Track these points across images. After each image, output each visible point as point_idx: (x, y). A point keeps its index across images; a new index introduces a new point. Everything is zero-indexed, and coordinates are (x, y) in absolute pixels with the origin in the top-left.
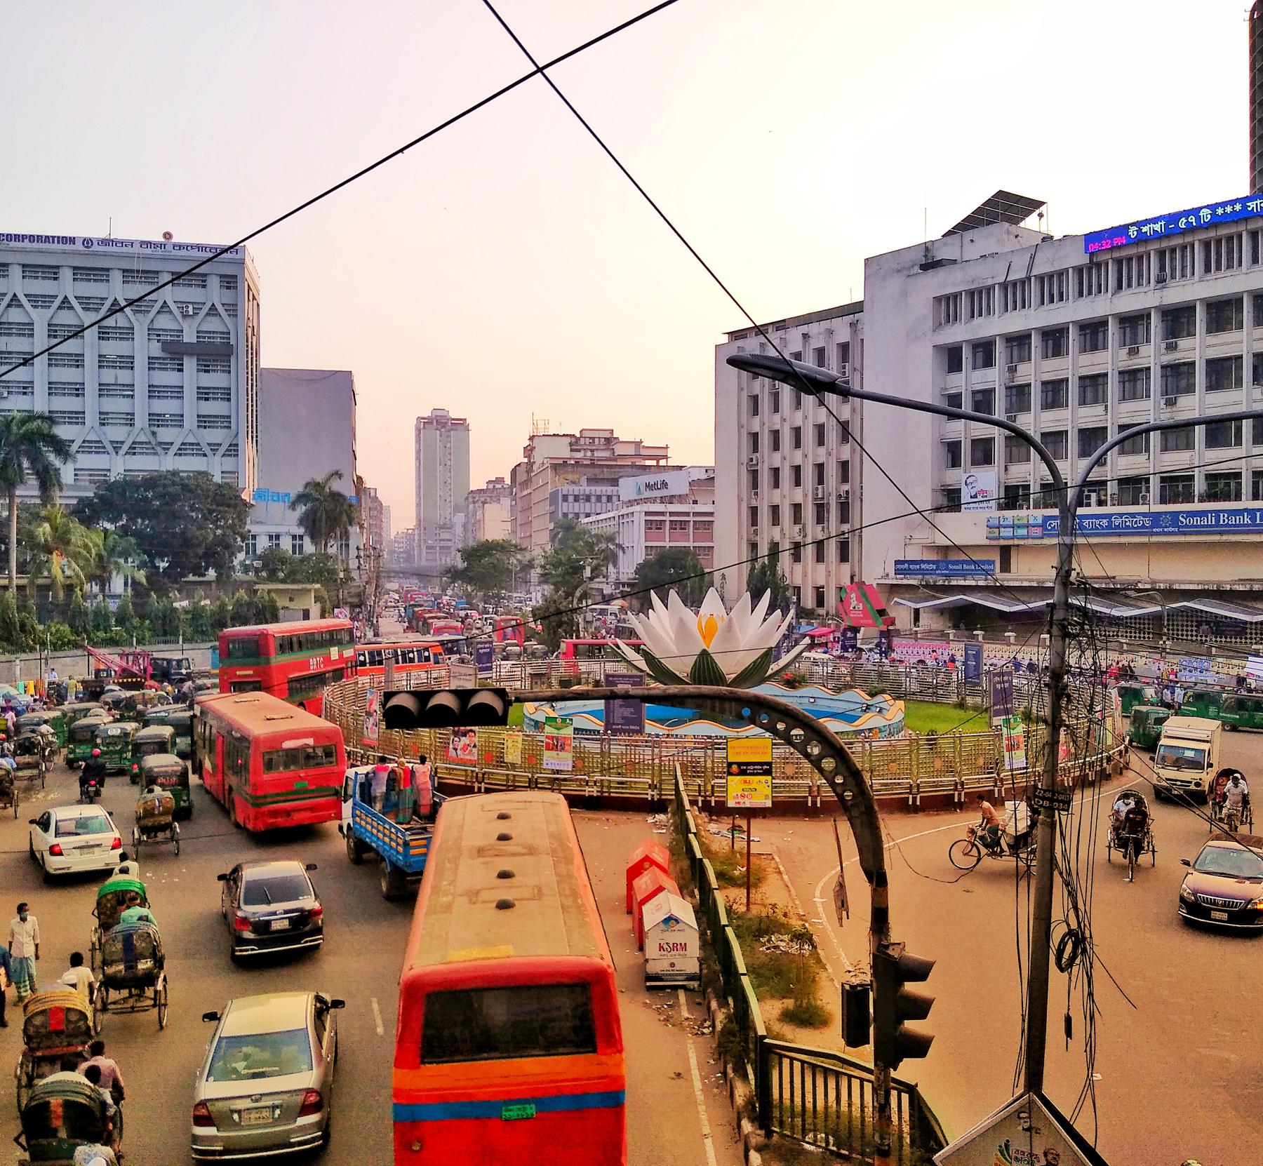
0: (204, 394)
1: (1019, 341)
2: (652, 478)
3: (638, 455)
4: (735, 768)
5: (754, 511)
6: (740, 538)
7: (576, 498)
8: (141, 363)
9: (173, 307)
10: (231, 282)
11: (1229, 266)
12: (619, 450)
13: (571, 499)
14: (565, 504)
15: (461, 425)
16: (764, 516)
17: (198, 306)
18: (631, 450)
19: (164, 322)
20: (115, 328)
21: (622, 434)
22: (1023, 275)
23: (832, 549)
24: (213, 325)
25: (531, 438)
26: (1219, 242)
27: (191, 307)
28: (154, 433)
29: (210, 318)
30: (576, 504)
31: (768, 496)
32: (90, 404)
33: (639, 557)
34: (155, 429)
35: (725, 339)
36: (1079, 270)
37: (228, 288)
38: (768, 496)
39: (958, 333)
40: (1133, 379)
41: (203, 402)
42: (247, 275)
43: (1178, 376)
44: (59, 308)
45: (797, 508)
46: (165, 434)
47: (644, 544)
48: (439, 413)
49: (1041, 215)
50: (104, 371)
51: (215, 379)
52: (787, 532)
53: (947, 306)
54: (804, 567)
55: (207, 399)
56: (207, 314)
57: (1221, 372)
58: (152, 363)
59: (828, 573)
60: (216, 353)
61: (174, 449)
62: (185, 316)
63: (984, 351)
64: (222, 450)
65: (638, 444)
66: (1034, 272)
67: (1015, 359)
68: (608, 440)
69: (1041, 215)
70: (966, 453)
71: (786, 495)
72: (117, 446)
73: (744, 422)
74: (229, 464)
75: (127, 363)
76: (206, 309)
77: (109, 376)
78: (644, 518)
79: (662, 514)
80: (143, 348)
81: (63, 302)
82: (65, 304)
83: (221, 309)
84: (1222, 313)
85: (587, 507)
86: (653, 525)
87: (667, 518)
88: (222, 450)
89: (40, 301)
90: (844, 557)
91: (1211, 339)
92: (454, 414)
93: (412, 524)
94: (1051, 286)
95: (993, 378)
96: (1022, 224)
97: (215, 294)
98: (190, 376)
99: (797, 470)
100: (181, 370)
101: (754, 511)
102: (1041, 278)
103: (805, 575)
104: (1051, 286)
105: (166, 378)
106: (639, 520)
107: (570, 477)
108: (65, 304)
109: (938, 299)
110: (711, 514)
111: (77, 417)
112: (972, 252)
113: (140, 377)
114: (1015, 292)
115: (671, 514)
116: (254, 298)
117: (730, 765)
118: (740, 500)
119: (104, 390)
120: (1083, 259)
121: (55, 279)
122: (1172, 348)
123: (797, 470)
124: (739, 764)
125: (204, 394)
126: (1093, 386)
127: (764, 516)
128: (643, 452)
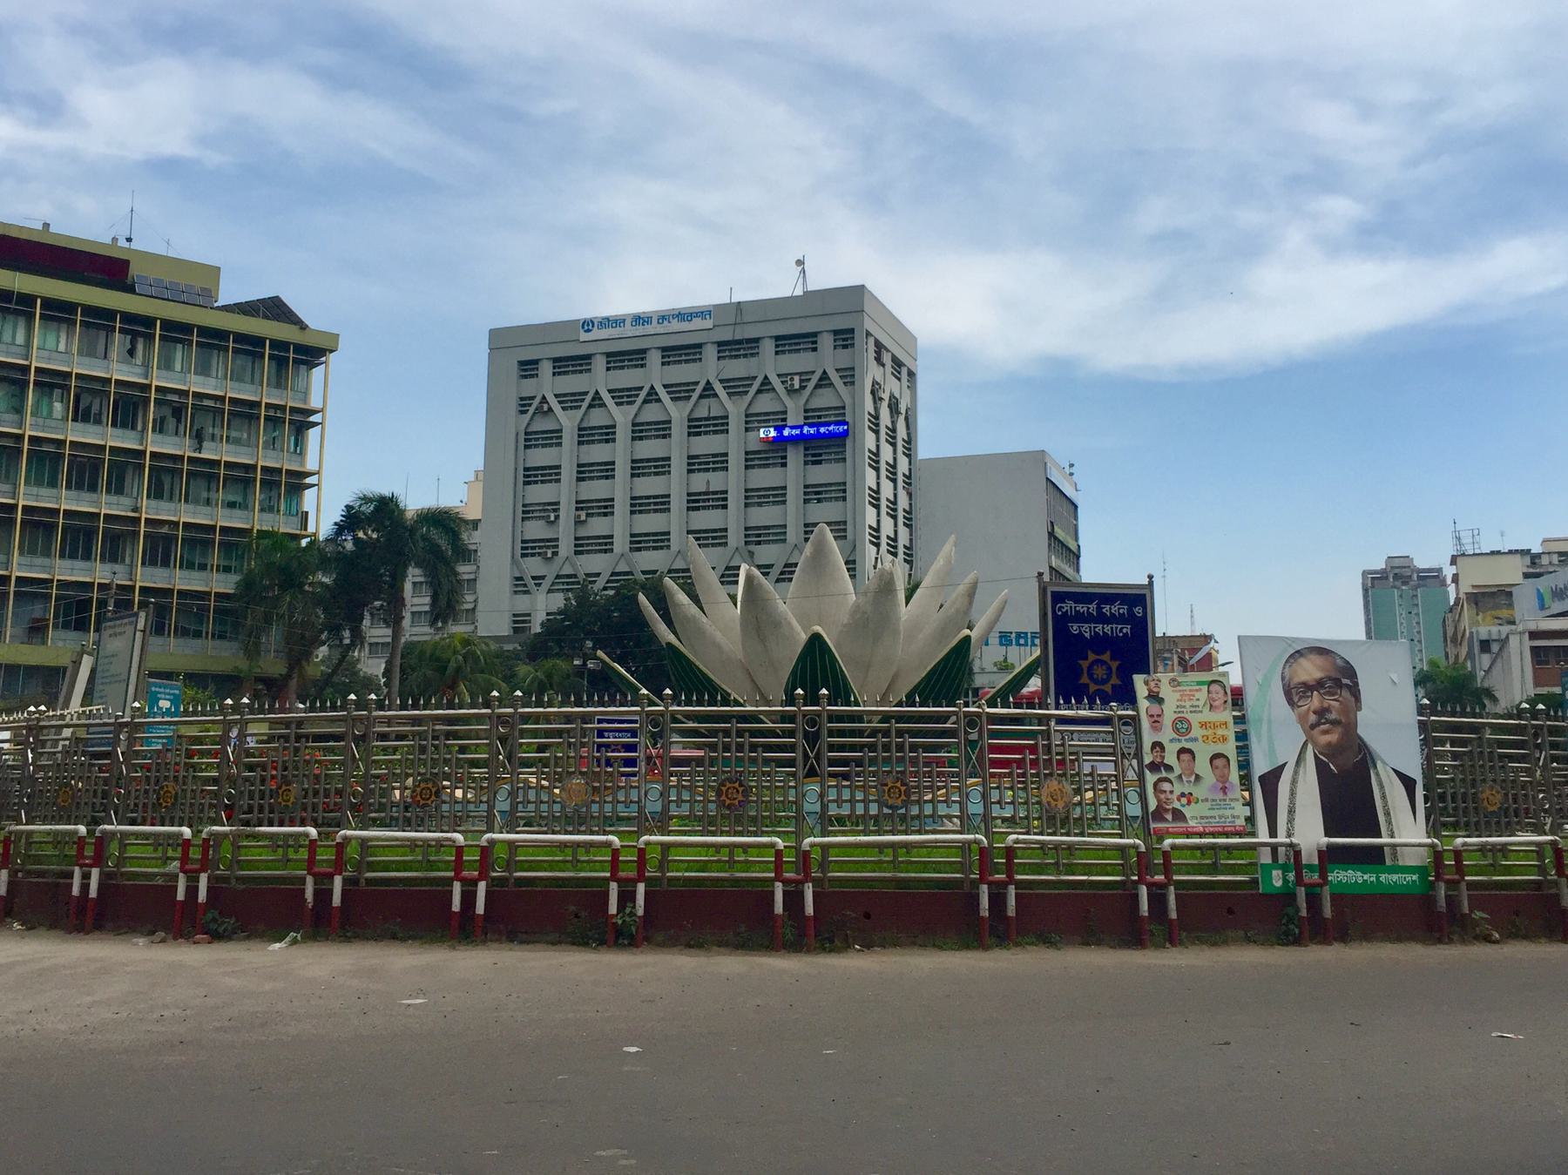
9: (776, 382)
10: (845, 338)
17: (805, 376)
19: (765, 404)
24: (824, 399)
27: (797, 378)
29: (820, 391)
34: (752, 547)
37: (845, 347)
42: (868, 325)
44: (645, 401)
50: (694, 476)
51: (823, 474)
55: (819, 501)
56: (817, 386)
58: (753, 460)
60: (826, 440)
62: (791, 391)
76: (815, 379)
77: (699, 482)
81: (649, 394)
83: (834, 377)
97: (828, 358)
98: (794, 473)
100: (784, 465)
105: (765, 478)
113: (733, 480)
116: (897, 363)
121: (642, 366)
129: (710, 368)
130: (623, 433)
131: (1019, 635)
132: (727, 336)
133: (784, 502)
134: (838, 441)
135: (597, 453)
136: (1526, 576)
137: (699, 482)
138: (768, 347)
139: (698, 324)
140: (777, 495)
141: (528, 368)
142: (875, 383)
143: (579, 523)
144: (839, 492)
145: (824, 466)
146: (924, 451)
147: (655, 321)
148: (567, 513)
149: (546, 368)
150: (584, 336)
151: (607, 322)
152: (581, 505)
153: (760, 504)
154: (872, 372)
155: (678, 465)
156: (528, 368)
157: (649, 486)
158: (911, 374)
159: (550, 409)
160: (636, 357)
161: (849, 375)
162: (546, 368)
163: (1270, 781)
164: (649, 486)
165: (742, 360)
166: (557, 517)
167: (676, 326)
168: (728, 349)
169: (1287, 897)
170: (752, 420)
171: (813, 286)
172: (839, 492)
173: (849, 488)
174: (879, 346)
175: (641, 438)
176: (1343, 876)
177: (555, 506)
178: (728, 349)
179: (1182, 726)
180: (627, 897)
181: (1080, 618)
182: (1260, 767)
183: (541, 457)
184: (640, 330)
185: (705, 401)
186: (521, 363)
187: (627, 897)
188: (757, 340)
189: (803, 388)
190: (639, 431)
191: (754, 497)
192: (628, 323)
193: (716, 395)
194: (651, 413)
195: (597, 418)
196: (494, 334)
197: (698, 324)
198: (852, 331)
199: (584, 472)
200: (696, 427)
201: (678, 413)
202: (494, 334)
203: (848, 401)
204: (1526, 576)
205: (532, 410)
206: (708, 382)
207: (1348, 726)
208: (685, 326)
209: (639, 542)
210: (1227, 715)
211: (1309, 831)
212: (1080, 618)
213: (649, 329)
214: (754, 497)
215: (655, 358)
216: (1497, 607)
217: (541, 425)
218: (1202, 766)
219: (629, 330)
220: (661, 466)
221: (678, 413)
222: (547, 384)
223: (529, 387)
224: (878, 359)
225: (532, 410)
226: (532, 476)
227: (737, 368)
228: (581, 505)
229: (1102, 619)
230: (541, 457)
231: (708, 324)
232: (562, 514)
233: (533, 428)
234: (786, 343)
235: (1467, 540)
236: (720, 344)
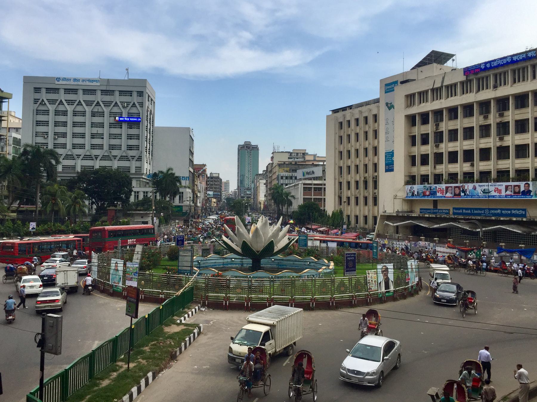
0: (130, 137)
1: (438, 113)
2: (308, 170)
3: (315, 160)
5: (340, 183)
6: (335, 195)
7: (287, 178)
8: (106, 125)
9: (119, 104)
10: (140, 94)
11: (524, 80)
12: (307, 158)
13: (284, 178)
15: (256, 148)
16: (345, 186)
17: (128, 103)
18: (312, 158)
19: (116, 110)
20: (98, 112)
21: (310, 151)
22: (439, 85)
23: (370, 201)
24: (134, 110)
25: (273, 153)
26: (519, 70)
28: (111, 152)
31: (346, 177)
32: (69, 141)
33: (301, 202)
34: (111, 150)
35: (331, 113)
36: (462, 83)
37: (140, 96)
38: (346, 177)
39: (416, 109)
40: (485, 131)
41: (129, 140)
42: (147, 91)
43: (503, 129)
44: (77, 105)
45: (357, 183)
46: (115, 152)
47: (302, 197)
48: (247, 143)
49: (453, 60)
51: (134, 131)
53: (410, 99)
54: (368, 208)
55: (131, 139)
56: (132, 106)
57: (522, 126)
58: (111, 125)
59: (369, 211)
60: (134, 122)
61: (118, 158)
62: (124, 107)
63: (425, 118)
64: (136, 158)
65: (315, 156)
66: (445, 84)
67: (439, 120)
68: (304, 154)
69: (453, 60)
70: (418, 160)
71: (353, 177)
72: (96, 157)
73: (337, 147)
74: (138, 164)
75: (102, 125)
76: (131, 104)
77: (95, 130)
78: (303, 186)
80: (107, 120)
82: (98, 104)
83: (137, 104)
84: (521, 100)
85: (287, 181)
86: (307, 189)
88: (136, 158)
89: (70, 102)
91: (517, 112)
92: (253, 144)
93: (236, 187)
94: (451, 89)
95: (429, 129)
96: (445, 65)
97: (135, 99)
98: (124, 130)
99: (357, 166)
101: (340, 183)
102: (447, 87)
103: (360, 210)
104: (451, 89)
106: (301, 187)
107: (286, 169)
108: (80, 104)
109: (407, 96)
111: (64, 146)
112: (422, 76)
114: (436, 92)
115: (315, 184)
116: (152, 100)
118: (335, 179)
119: (93, 136)
120: (463, 78)
122: (501, 115)
123: (357, 166)
125: (130, 137)
126: (469, 133)
127: (345, 186)
128: (317, 159)
129: (99, 97)
130: (70, 113)
131: (183, 177)
132: (104, 88)
133: (121, 138)
134: (138, 123)
135: (61, 118)
136: (289, 158)
137: (95, 130)
138: (117, 93)
139: (94, 84)
140: (118, 136)
141: (37, 90)
142: (148, 107)
143: (55, 139)
144: (138, 137)
145: (133, 129)
146: (156, 125)
147: (81, 81)
148: (51, 135)
149: (44, 91)
150: (57, 82)
151: (64, 79)
152: (56, 134)
153: (113, 138)
154: (147, 104)
155: (88, 124)
156: (37, 90)
157: (78, 130)
158: (154, 102)
159: (45, 104)
160: (74, 91)
161: (142, 104)
162: (44, 91)
163: (380, 283)
164: (78, 130)
165: (108, 96)
166: (48, 137)
167: (88, 83)
168: (105, 92)
169: (381, 298)
170: (111, 114)
171: (131, 77)
172: (138, 137)
173: (140, 136)
174: (149, 96)
175: (76, 116)
176: (387, 294)
177: (47, 133)
178: (105, 92)
179: (371, 277)
180: (313, 304)
181: (349, 257)
182: (379, 282)
183: (41, 118)
184: (76, 83)
185: (97, 107)
186: (35, 88)
187: (313, 304)
188: (113, 91)
189: (127, 106)
190: (75, 114)
191: (112, 136)
192: (72, 80)
193: (100, 105)
194: (79, 108)
195: (61, 108)
196: (25, 78)
197: (94, 84)
198: (143, 92)
199: (56, 124)
200: (93, 114)
201: (88, 110)
202: (25, 78)
203: (141, 112)
204: (289, 158)
205: (39, 103)
206: (98, 103)
207: (387, 276)
208: (91, 84)
209: (74, 146)
210: (376, 276)
211: (383, 290)
212: (349, 257)
213: (80, 83)
214: (112, 136)
215: (80, 92)
216: (284, 167)
217: (42, 108)
218: (373, 282)
219: (72, 82)
220: (83, 125)
221: (88, 110)
222: (44, 96)
223: (37, 96)
224: (148, 101)
225: (39, 103)
226: (38, 123)
227: (107, 98)
228: (56, 134)
229: (351, 257)
230: (41, 118)
231: (98, 84)
232: (49, 136)
233: (38, 109)
234: (122, 93)
235: (276, 148)
236: (102, 90)
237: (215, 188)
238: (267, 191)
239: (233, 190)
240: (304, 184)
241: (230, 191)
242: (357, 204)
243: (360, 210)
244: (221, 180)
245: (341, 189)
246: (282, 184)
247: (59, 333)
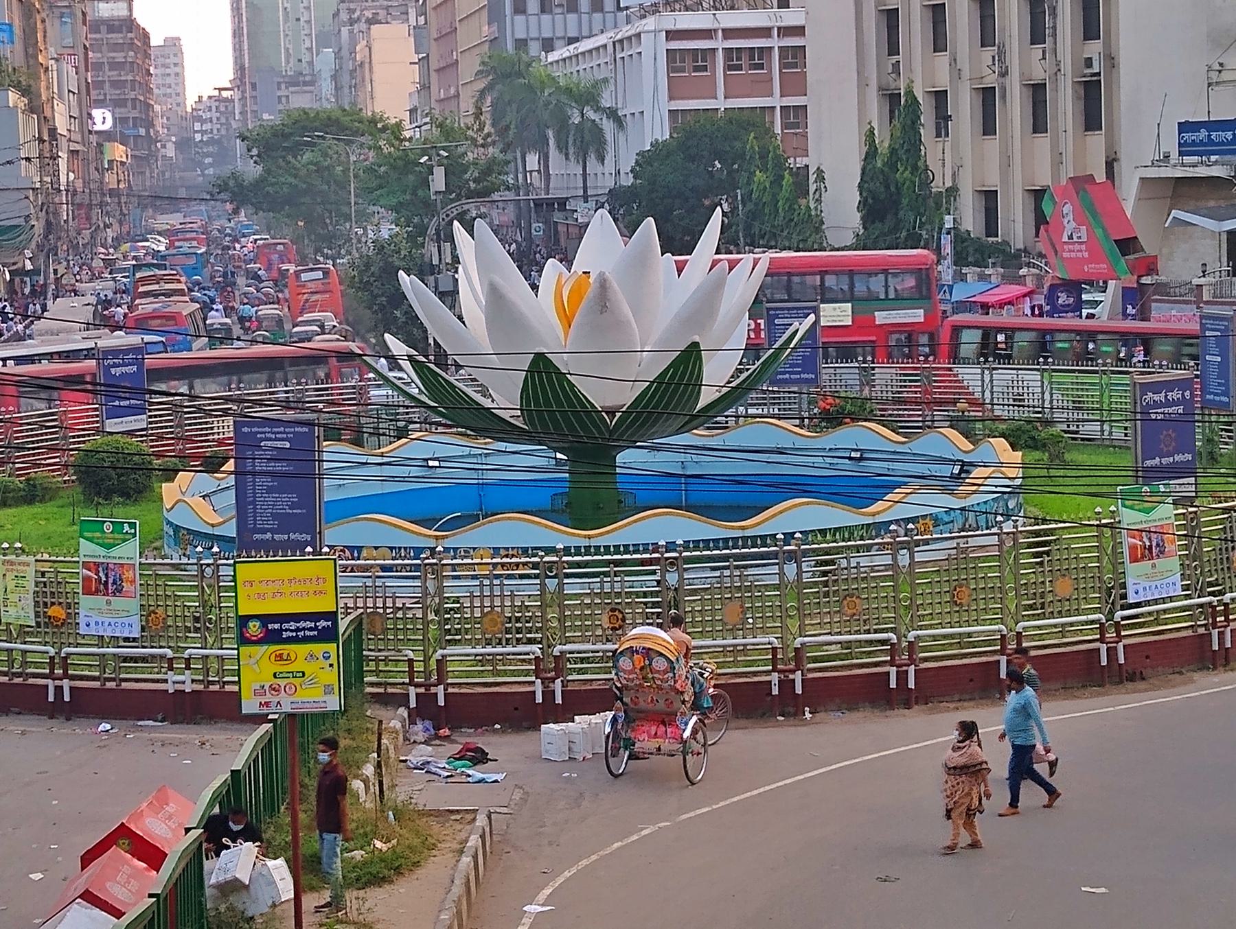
4: (254, 628)
6: (862, 84)
14: (520, 19)
23: (1065, 105)
30: (546, 18)
47: (666, 106)
52: (964, 63)
78: (664, 45)
79: (707, 34)
86: (687, 63)
87: (719, 44)
90: (1092, 120)
93: (224, 74)
106: (653, 50)
110: (799, 31)
115: (729, 33)
117: (244, 620)
124: (265, 619)
237: (115, 84)
238: (425, 87)
239: (208, 91)
240: (671, 35)
241: (190, 101)
242: (988, 128)
243: (1006, 162)
244: (146, 36)
245: (893, 49)
246: (522, 44)
247: (176, 875)
